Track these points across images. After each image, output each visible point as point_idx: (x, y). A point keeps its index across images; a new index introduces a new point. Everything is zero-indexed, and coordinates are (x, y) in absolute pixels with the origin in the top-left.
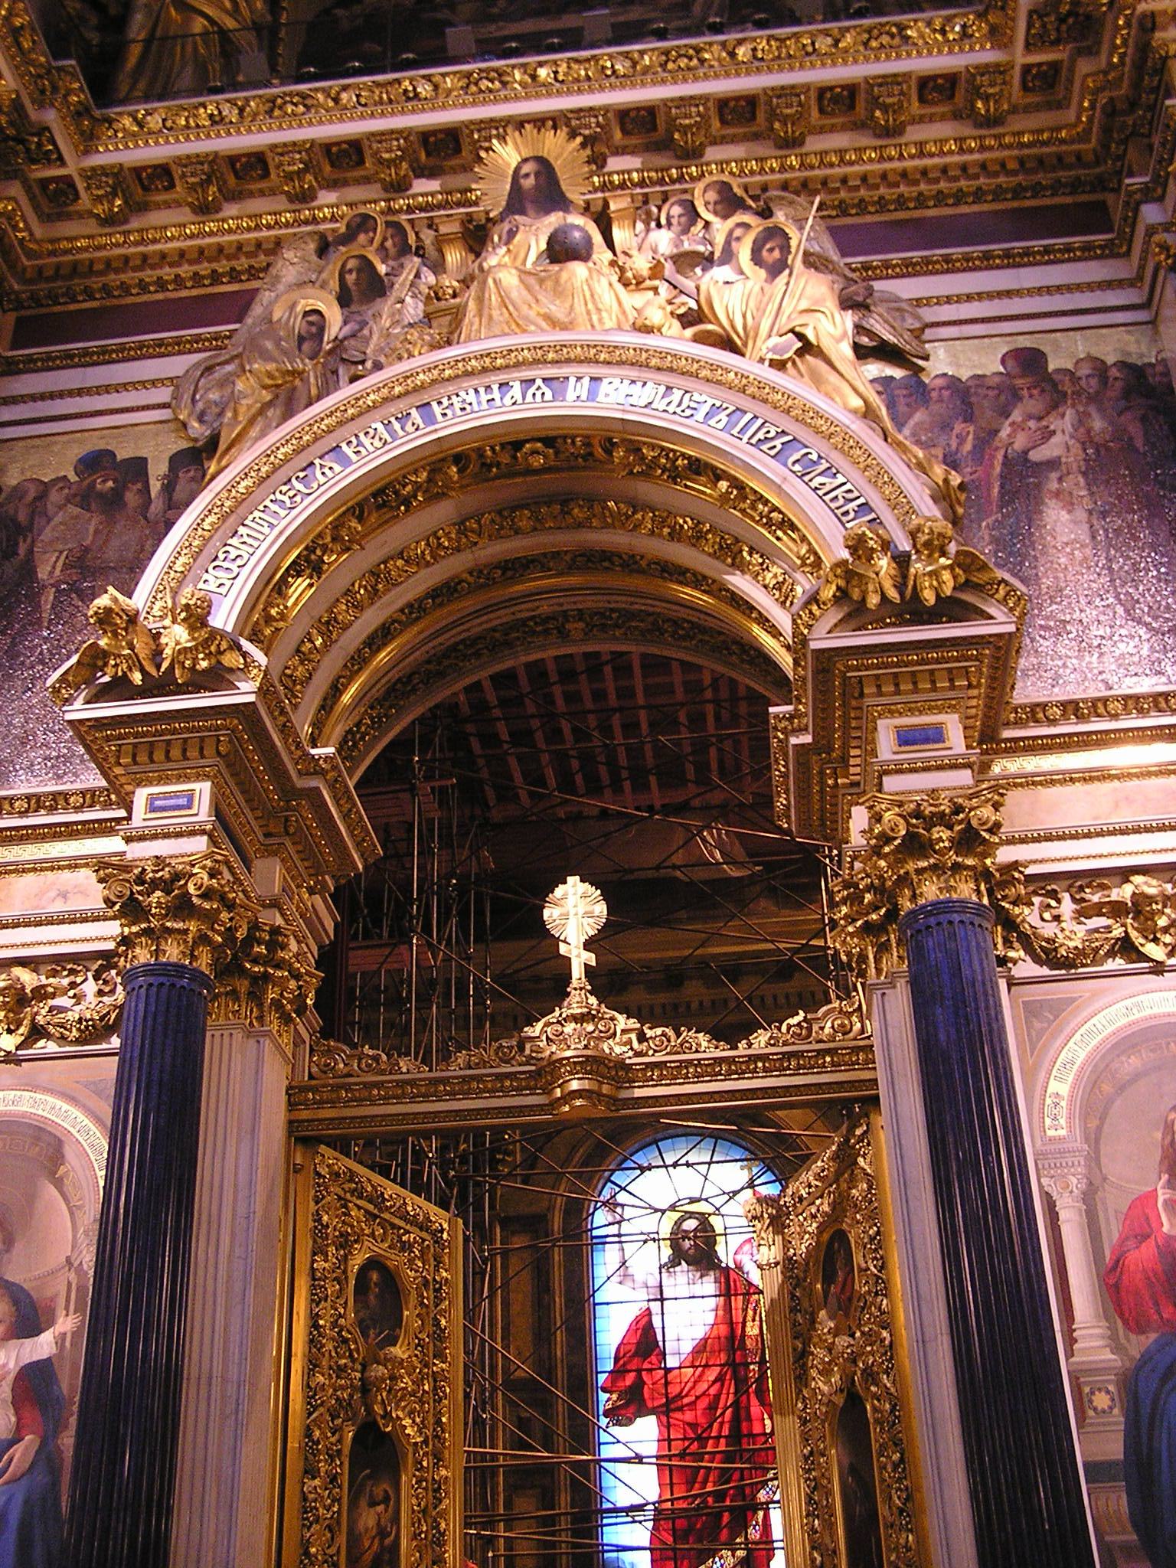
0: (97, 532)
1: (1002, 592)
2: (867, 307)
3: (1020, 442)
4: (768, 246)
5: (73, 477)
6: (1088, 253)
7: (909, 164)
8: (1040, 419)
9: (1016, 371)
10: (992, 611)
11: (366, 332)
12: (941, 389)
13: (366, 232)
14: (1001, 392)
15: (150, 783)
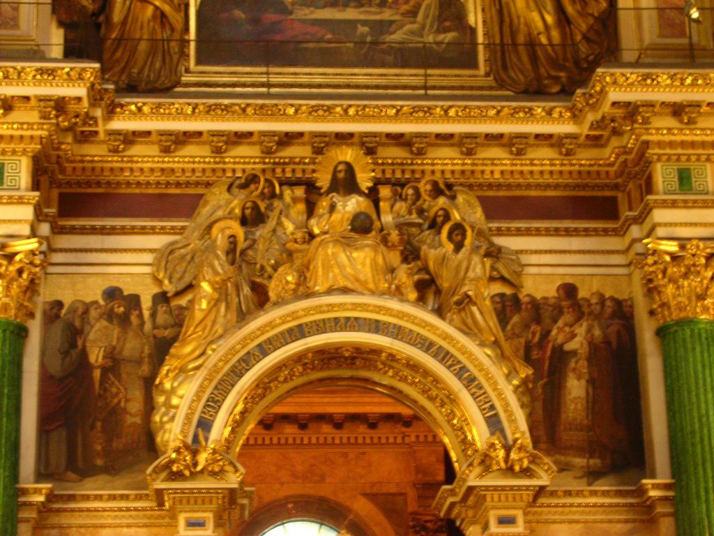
0: (118, 339)
1: (546, 467)
2: (498, 258)
3: (560, 340)
4: (456, 232)
5: (102, 302)
6: (606, 232)
7: (526, 169)
8: (571, 326)
9: (563, 296)
10: (541, 473)
11: (256, 246)
12: (527, 303)
13: (255, 183)
14: (555, 309)
15: (186, 511)
